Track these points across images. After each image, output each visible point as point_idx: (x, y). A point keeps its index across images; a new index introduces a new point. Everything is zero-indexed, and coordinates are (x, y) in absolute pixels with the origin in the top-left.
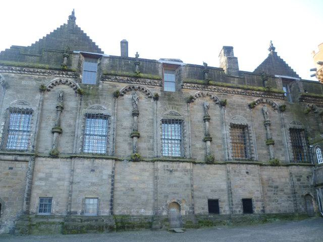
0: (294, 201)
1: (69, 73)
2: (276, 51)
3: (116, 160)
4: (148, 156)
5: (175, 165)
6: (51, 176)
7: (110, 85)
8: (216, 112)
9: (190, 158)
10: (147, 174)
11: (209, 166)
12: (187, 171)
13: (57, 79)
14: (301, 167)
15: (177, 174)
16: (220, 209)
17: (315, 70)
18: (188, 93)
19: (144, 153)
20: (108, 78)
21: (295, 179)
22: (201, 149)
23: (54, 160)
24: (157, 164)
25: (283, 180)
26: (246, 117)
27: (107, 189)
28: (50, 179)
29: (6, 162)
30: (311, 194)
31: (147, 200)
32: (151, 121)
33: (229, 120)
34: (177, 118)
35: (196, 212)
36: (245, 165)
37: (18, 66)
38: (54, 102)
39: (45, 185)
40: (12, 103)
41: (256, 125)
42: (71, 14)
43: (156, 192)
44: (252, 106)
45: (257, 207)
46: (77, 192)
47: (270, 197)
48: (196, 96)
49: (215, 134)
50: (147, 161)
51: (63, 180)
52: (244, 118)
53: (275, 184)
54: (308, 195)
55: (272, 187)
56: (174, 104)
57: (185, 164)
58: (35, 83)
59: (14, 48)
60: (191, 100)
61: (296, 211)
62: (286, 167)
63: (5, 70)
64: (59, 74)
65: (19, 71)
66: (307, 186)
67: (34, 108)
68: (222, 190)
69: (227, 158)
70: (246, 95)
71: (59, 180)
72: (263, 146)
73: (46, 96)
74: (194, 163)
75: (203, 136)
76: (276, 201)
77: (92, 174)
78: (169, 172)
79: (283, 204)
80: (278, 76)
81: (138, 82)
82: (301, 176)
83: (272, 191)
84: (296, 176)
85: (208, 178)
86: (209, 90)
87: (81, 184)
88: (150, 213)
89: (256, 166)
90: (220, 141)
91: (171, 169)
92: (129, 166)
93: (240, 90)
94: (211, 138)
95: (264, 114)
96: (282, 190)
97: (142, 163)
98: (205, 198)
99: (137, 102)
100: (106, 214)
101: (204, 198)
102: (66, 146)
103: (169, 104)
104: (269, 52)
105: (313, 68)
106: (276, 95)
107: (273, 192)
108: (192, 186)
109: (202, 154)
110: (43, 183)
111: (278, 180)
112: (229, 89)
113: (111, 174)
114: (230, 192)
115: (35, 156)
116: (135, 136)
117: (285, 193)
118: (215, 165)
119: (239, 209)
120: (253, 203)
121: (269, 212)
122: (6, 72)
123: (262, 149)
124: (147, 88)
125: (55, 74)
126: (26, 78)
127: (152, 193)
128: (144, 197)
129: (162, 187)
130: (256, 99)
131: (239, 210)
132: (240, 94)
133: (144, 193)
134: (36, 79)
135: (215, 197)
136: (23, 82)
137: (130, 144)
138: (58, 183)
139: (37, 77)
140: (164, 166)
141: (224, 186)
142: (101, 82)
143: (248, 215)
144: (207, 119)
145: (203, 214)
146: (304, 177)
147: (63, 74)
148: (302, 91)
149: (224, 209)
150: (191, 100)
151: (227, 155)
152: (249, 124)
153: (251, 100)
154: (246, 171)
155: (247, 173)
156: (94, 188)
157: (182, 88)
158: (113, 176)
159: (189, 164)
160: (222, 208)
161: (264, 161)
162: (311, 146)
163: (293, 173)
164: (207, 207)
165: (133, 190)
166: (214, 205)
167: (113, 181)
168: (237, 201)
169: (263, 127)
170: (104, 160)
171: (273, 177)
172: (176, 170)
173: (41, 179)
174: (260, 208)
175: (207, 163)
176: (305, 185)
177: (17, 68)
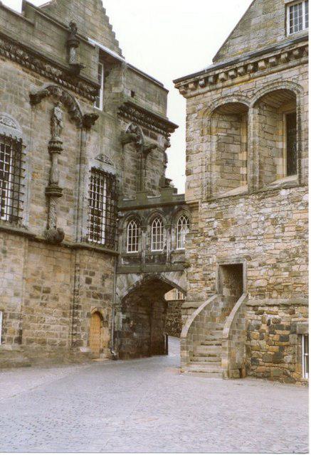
0: (73, 323)
26: (22, 121)
41: (36, 144)
44: (35, 100)
52: (17, 124)
53: (47, 284)
62: (69, 251)
70: (30, 68)
72: (38, 196)
79: (53, 327)
83: (38, 297)
84: (86, 273)
89: (23, 240)
95: (52, 124)
96: (56, 299)
106: (85, 86)
117: (59, 306)
123: (37, 203)
176: (97, 292)
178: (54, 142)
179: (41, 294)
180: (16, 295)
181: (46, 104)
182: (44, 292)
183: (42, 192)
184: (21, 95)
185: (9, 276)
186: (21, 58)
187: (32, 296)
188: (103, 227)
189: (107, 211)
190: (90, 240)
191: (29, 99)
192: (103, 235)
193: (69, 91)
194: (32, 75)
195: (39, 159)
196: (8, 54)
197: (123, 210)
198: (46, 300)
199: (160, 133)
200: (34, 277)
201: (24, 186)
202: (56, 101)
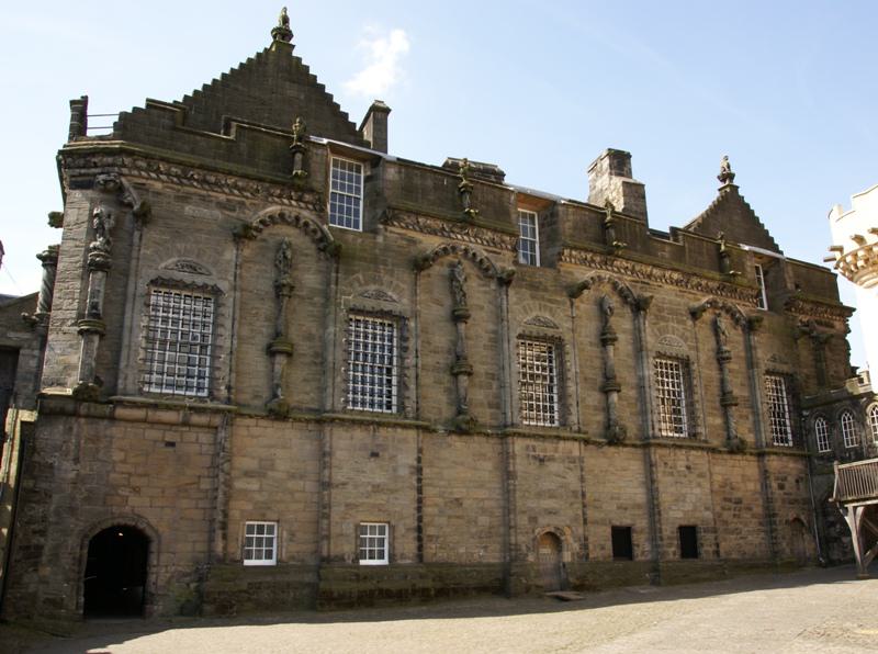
1: (307, 197)
2: (735, 182)
5: (549, 445)
6: (272, 467)
7: (402, 239)
9: (579, 431)
10: (488, 465)
11: (612, 449)
12: (574, 462)
13: (273, 209)
14: (785, 458)
15: (553, 467)
16: (636, 548)
17: (841, 249)
21: (775, 485)
22: (596, 408)
23: (277, 424)
24: (513, 443)
25: (751, 486)
26: (686, 340)
27: (405, 502)
28: (270, 473)
29: (156, 426)
30: (802, 517)
31: (490, 528)
32: (492, 336)
34: (550, 332)
35: (591, 556)
37: (180, 164)
38: (266, 271)
39: (261, 490)
40: (163, 265)
42: (277, 23)
43: (508, 509)
44: (695, 314)
46: (342, 508)
49: (625, 375)
50: (487, 435)
51: (302, 477)
53: (738, 495)
54: (797, 520)
55: (730, 500)
56: (543, 298)
57: (569, 444)
58: (217, 213)
59: (152, 104)
60: (575, 291)
61: (775, 554)
63: (139, 169)
64: (280, 196)
65: (176, 176)
66: (796, 501)
67: (224, 285)
71: (292, 476)
73: (247, 252)
74: (587, 442)
76: (737, 531)
77: (373, 463)
78: (538, 463)
79: (750, 538)
80: (747, 248)
82: (785, 479)
83: (729, 509)
84: (777, 479)
87: (350, 487)
88: (491, 555)
90: (633, 393)
91: (542, 454)
92: (450, 446)
93: (676, 276)
96: (750, 509)
97: (476, 438)
98: (606, 525)
100: (408, 561)
102: (300, 394)
103: (533, 297)
105: (837, 244)
107: (732, 512)
108: (583, 495)
109: (598, 422)
110: (254, 485)
111: (741, 485)
113: (415, 463)
114: (653, 508)
115: (232, 413)
118: (626, 449)
119: (673, 549)
120: (699, 535)
122: (140, 176)
124: (485, 254)
125: (272, 195)
126: (195, 198)
127: (498, 512)
128: (484, 520)
129: (524, 496)
130: (705, 300)
131: (672, 551)
134: (221, 206)
135: (626, 522)
136: (188, 209)
137: (448, 391)
138: (291, 485)
139: (222, 197)
140: (528, 447)
141: (639, 495)
142: (381, 226)
143: (690, 562)
145: (601, 559)
146: (791, 480)
147: (290, 198)
148: (790, 286)
149: (642, 545)
150: (575, 291)
151: (650, 428)
152: (692, 354)
155: (688, 468)
156: (380, 499)
158: (419, 470)
159: (576, 444)
160: (638, 546)
161: (715, 443)
162: (805, 413)
163: (771, 470)
164: (609, 545)
165: (461, 504)
166: (622, 538)
167: (419, 480)
168: (669, 530)
169: (715, 365)
170: (399, 430)
171: (733, 480)
172: (552, 459)
173: (248, 474)
176: (792, 497)
177: (174, 170)
179: (733, 506)
180: (707, 509)
181: (707, 316)
183: (718, 404)
184: (681, 314)
185: (698, 491)
187: (723, 508)
189: (789, 412)
190: (775, 444)
191: (690, 316)
192: (790, 437)
197: (807, 409)
202: (717, 312)
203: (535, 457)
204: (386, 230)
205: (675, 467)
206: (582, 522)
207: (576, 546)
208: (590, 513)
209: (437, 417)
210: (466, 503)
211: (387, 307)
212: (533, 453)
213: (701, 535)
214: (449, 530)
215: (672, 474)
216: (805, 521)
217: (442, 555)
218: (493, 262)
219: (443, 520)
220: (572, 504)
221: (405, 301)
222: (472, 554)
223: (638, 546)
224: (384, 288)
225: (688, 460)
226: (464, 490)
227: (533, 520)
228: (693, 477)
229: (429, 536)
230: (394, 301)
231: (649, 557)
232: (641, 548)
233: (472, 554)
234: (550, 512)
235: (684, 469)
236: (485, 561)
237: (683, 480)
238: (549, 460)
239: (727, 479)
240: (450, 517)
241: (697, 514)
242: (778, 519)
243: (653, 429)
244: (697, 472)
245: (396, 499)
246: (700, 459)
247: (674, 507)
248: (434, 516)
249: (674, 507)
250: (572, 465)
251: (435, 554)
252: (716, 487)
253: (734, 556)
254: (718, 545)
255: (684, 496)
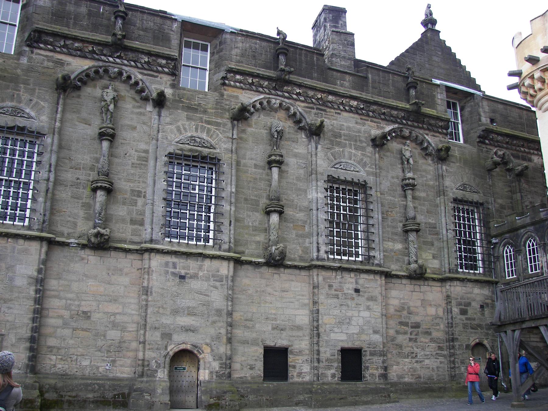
0: (450, 356)
3: (51, 243)
4: (129, 237)
5: (192, 264)
7: (48, 60)
8: (298, 148)
11: (271, 270)
14: (470, 285)
15: (195, 284)
16: (290, 369)
18: (237, 97)
19: (122, 231)
20: (46, 43)
21: (456, 310)
24: (150, 259)
25: (432, 311)
26: (364, 165)
30: (485, 342)
31: (120, 342)
33: (323, 165)
34: (206, 151)
35: (235, 375)
36: (352, 275)
41: (386, 185)
44: (379, 143)
45: (372, 369)
47: (401, 347)
48: (254, 107)
52: (359, 168)
53: (415, 319)
54: (479, 345)
55: (406, 324)
56: (201, 120)
57: (216, 263)
61: (453, 377)
62: (439, 284)
66: (480, 326)
68: (299, 328)
69: (315, 254)
70: (368, 115)
72: (396, 234)
75: (264, 202)
76: (412, 355)
78: (177, 280)
79: (427, 362)
80: (438, 82)
81: (118, 60)
82: (469, 304)
83: (405, 333)
84: (459, 304)
85: (269, 298)
86: (286, 94)
89: (377, 277)
91: (183, 272)
92: (83, 259)
94: (282, 207)
95: (402, 163)
96: (428, 333)
97: (113, 253)
98: (257, 345)
99: (112, 107)
101: (254, 343)
103: (189, 118)
104: (423, 30)
106: (433, 122)
107: (409, 336)
108: (230, 314)
109: (259, 242)
111: (421, 310)
112: (330, 98)
114: (316, 332)
116: (101, 188)
117: (432, 340)
118: (287, 271)
119: (333, 371)
120: (364, 358)
121: (395, 379)
123: (394, 240)
124: (140, 76)
127: (132, 327)
128: (114, 334)
129: (158, 312)
130: (388, 128)
131: (332, 373)
132: (356, 111)
133: (115, 325)
135: (281, 342)
137: (87, 206)
140: (167, 264)
141: (303, 317)
144: (275, 162)
146: (476, 305)
148: (485, 120)
149: (301, 369)
151: (315, 249)
152: (371, 180)
153: (378, 128)
154: (354, 286)
155: (357, 291)
157: (224, 84)
159: (225, 264)
160: (294, 367)
161: (394, 268)
162: (494, 241)
163: (453, 295)
164: (260, 365)
165: (89, 318)
166: (276, 361)
168: (329, 352)
170: (21, 241)
171: (411, 304)
172: (195, 277)
174: (377, 369)
175: (268, 264)
178: (406, 179)
179: (410, 330)
180: (375, 332)
182: (412, 327)
184: (361, 141)
185: (366, 314)
186: (356, 108)
187: (397, 332)
188: (480, 257)
189: (481, 240)
190: (460, 270)
191: (371, 144)
192: (480, 264)
193: (416, 130)
194: (372, 121)
195: (392, 198)
196: (342, 108)
197: (496, 236)
198: (416, 335)
199: (533, 154)
200: (399, 313)
201: (373, 225)
203: (174, 274)
204: (32, 52)
205: (341, 290)
206: (224, 340)
207: (216, 365)
208: (239, 333)
209: (71, 231)
210: (95, 317)
211: (21, 122)
212: (173, 270)
213: (366, 358)
214: (71, 342)
215: (337, 297)
216: (488, 346)
217: (61, 366)
218: (148, 84)
219: (67, 332)
220: (214, 322)
221: (44, 118)
222: (98, 368)
223: (294, 367)
224: (22, 106)
225: (357, 283)
226: (94, 304)
227: (167, 336)
228: (361, 300)
229: (49, 347)
230: (32, 118)
231: (307, 378)
232: (297, 370)
233: (98, 368)
234: (188, 330)
235: (353, 292)
236: (111, 375)
237: (349, 302)
238: (191, 277)
239: (403, 304)
240: (74, 329)
241: (364, 337)
242: (457, 344)
243: (318, 251)
244: (366, 295)
245: (9, 308)
246: (373, 285)
247: (336, 330)
248: (58, 327)
249: (336, 330)
250: (218, 284)
251: (55, 366)
252: (392, 310)
253: (406, 380)
254: (386, 369)
255: (350, 319)
